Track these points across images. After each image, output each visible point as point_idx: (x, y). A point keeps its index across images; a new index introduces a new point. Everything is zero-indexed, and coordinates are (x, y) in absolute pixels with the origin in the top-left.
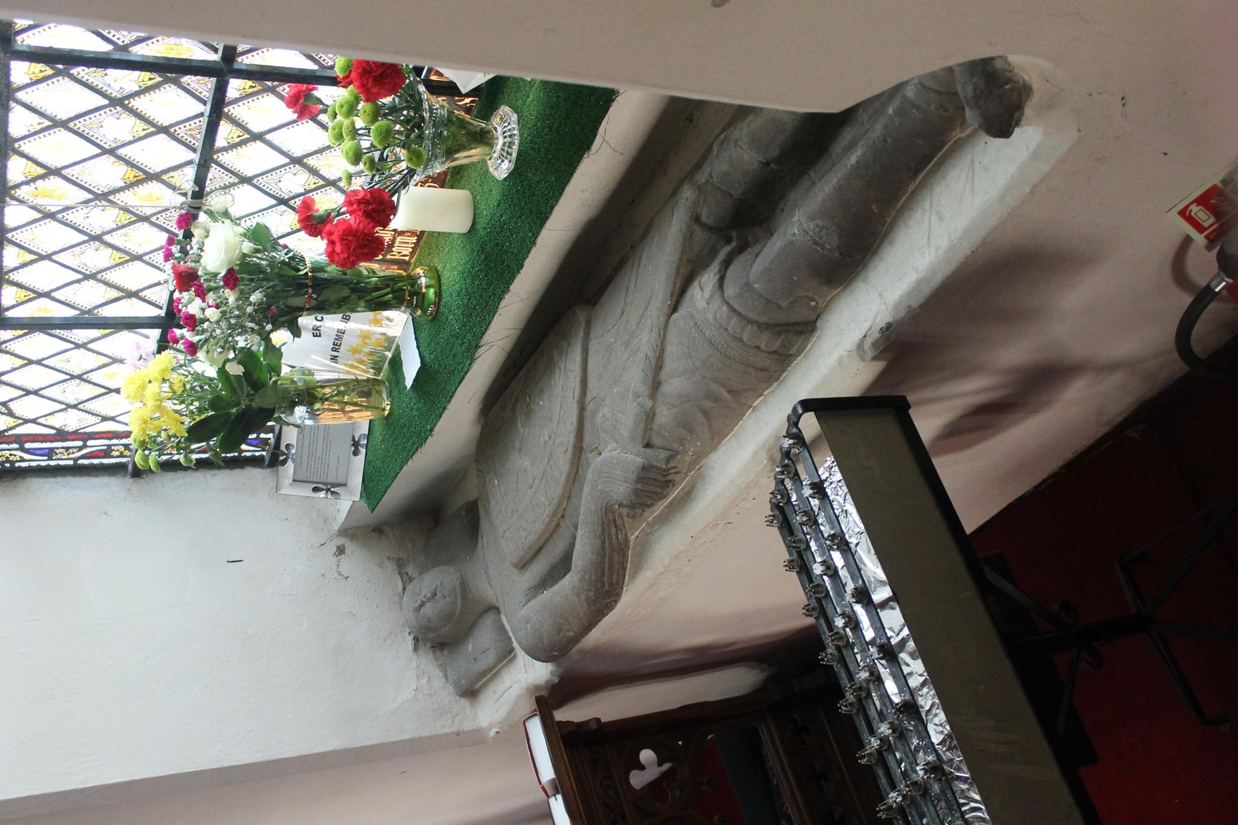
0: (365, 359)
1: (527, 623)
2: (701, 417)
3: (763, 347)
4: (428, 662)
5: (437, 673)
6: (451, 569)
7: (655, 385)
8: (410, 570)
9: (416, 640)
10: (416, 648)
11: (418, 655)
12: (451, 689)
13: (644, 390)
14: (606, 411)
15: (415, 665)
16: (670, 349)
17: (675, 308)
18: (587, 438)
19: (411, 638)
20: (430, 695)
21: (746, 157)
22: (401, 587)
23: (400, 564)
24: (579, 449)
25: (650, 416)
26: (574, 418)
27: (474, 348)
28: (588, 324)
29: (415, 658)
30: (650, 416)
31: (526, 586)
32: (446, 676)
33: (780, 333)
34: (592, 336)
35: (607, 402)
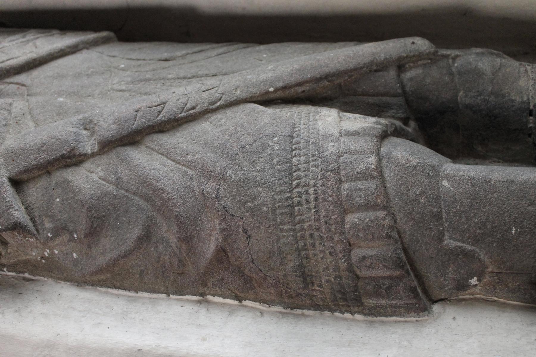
2: (136, 232)
3: (357, 253)
7: (132, 138)
13: (108, 128)
14: (19, 105)
16: (205, 128)
21: (522, 83)
25: (72, 159)
28: (106, 41)
30: (72, 159)
33: (399, 265)
34: (101, 49)
35: (33, 100)
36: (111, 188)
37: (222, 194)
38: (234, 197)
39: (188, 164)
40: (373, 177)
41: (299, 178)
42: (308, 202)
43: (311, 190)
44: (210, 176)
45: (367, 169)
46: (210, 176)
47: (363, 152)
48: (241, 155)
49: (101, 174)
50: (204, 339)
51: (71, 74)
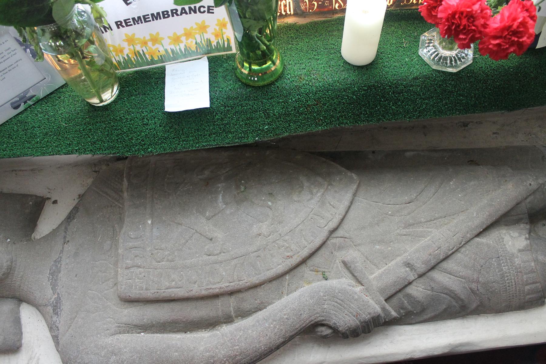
0: (126, 52)
17: (478, 235)
18: (317, 260)
24: (304, 261)
26: (318, 242)
31: (124, 320)
36: (429, 292)
37: (479, 288)
38: (484, 288)
39: (461, 277)
40: (534, 272)
41: (507, 276)
42: (512, 285)
43: (513, 281)
44: (473, 282)
45: (532, 269)
46: (473, 282)
47: (528, 261)
48: (482, 270)
49: (423, 287)
50: (471, 333)
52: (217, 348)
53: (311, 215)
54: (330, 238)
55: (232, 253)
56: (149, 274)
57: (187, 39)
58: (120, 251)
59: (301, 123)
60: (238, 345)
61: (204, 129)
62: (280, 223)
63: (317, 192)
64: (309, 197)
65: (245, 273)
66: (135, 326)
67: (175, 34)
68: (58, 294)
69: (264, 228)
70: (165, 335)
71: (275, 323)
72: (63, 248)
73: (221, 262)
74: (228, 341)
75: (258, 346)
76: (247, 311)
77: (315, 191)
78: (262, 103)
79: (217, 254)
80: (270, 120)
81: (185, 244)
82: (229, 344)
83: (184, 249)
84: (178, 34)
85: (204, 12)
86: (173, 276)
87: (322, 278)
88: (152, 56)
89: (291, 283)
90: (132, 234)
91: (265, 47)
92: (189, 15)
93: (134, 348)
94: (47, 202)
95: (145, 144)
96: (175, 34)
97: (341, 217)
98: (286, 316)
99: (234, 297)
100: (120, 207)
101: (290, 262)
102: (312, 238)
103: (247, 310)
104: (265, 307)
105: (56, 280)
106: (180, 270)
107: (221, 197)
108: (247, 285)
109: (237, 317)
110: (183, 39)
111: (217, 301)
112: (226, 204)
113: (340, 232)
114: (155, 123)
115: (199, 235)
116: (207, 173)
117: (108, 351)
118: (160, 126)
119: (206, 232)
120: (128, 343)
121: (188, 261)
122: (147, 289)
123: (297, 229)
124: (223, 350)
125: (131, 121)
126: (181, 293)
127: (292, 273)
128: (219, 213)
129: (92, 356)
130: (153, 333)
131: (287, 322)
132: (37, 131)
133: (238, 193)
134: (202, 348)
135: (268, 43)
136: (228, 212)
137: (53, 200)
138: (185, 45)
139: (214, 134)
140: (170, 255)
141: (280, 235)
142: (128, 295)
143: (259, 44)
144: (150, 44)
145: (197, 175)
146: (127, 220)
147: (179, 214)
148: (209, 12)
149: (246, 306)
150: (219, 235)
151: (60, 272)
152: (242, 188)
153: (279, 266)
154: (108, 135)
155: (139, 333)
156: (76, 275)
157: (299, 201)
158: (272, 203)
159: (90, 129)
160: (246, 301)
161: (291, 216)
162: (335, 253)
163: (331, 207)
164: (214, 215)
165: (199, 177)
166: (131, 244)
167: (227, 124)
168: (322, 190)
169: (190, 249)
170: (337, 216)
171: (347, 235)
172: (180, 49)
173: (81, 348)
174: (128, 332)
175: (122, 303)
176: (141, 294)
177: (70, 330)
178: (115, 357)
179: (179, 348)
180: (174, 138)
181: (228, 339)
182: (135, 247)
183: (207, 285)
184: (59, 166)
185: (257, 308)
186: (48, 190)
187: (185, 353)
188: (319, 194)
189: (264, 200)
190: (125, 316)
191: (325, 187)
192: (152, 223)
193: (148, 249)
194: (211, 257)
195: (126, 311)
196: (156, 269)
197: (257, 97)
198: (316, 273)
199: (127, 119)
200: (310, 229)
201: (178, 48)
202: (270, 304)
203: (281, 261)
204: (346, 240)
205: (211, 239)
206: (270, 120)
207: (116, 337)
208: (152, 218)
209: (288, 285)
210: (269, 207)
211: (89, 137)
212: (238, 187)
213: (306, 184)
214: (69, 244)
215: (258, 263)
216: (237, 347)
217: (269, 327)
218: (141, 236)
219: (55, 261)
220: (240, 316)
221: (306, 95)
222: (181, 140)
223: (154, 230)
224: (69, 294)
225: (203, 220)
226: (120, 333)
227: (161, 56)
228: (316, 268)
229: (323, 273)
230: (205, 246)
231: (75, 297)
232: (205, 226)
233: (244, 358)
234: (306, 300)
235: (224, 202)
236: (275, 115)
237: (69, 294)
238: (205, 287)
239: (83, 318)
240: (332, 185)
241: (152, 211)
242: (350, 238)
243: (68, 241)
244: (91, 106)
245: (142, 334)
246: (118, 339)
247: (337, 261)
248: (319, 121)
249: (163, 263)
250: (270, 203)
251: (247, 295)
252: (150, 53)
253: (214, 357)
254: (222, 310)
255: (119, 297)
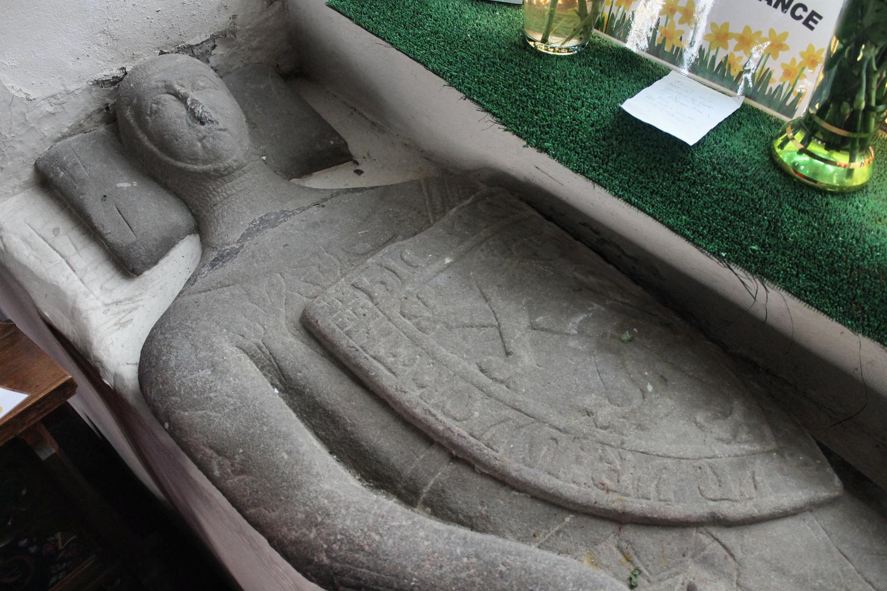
1: (213, 366)
4: (82, 104)
5: (66, 124)
6: (247, 142)
8: (219, 51)
9: (116, 81)
10: (97, 83)
11: (90, 91)
12: (43, 150)
15: (72, 88)
19: (119, 74)
20: (25, 124)
22: (192, 42)
23: (224, 37)
24: (620, 519)
26: (677, 510)
27: (761, 268)
29: (84, 85)
31: (277, 346)
32: (64, 137)
51: (794, 573)
52: (348, 508)
53: (702, 462)
54: (701, 529)
55: (520, 398)
56: (374, 319)
57: (737, 49)
58: (370, 260)
59: (821, 289)
60: (381, 535)
61: (653, 177)
62: (640, 427)
63: (746, 442)
64: (726, 436)
65: (509, 443)
66: (280, 369)
67: (726, 25)
68: (242, 246)
69: (606, 413)
70: (301, 425)
71: (474, 560)
72: (309, 207)
73: (489, 395)
74: (375, 514)
75: (409, 570)
76: (450, 509)
77: (744, 436)
78: (780, 206)
79: (495, 380)
80: (774, 242)
81: (465, 326)
82: (371, 521)
83: (456, 331)
84: (731, 30)
85: (800, 17)
86: (400, 350)
87: (626, 577)
88: (664, 40)
89: (564, 533)
90: (408, 254)
91: (863, 105)
92: (771, 8)
93: (245, 388)
94: (350, 163)
95: (547, 133)
96: (726, 25)
97: (756, 512)
98: (503, 568)
99: (455, 466)
100: (429, 222)
101: (598, 495)
102: (671, 496)
103: (453, 506)
104: (484, 531)
105: (258, 230)
106: (420, 349)
107: (581, 318)
108: (493, 462)
109: (427, 503)
110: (732, 43)
111: (423, 449)
112: (581, 332)
113: (730, 537)
114: (589, 116)
115: (498, 334)
116: (592, 279)
117: (211, 357)
118: (592, 125)
119: (511, 338)
120: (246, 376)
121: (443, 350)
122: (348, 333)
123: (659, 461)
124: (353, 520)
125: (558, 90)
126: (387, 381)
127: (583, 520)
128: (557, 333)
129: (188, 346)
130: (290, 405)
131: (494, 579)
132: (429, 23)
133: (613, 337)
134: (326, 487)
135: (873, 103)
136: (572, 343)
137: (360, 168)
138: (726, 57)
139: (661, 196)
140: (428, 319)
141: (623, 443)
142: (317, 317)
143: (860, 86)
144: (678, 16)
145: (576, 270)
146: (422, 236)
147: (499, 286)
148: (806, 23)
149: (459, 499)
150: (527, 358)
151: (273, 227)
152: (626, 336)
153: (574, 486)
154: (510, 85)
155: (274, 385)
156: (286, 245)
157: (701, 427)
158: (655, 391)
159: (494, 63)
160: (466, 490)
161: (668, 435)
162: (689, 561)
163: (751, 480)
164: (546, 330)
165: (575, 273)
166: (393, 263)
167: (695, 196)
168: (757, 447)
169: (464, 338)
170: (750, 504)
171: (739, 554)
172: (714, 58)
173: (189, 323)
174: (262, 369)
175: (299, 326)
176: (334, 331)
177: (203, 294)
178: (209, 373)
179: (298, 452)
180: (595, 157)
181: (378, 512)
182: (394, 272)
183: (436, 406)
184: (408, 142)
185: (470, 518)
186: (365, 154)
187: (297, 468)
188: (746, 447)
189: (645, 377)
190: (283, 343)
191: (768, 448)
192: (449, 265)
193: (408, 288)
194: (481, 374)
195: (290, 339)
196: (390, 320)
197: (778, 191)
198: (624, 560)
199: (555, 84)
200: (682, 480)
201: (713, 53)
202: (496, 532)
203: (583, 480)
204: (730, 559)
205: (508, 354)
206: (774, 242)
207: (243, 356)
208: (456, 260)
209: (558, 532)
210: (644, 392)
211: (484, 71)
212: (621, 329)
213: (737, 416)
214: (321, 209)
215: (545, 448)
216: (377, 538)
217: (458, 559)
218: (417, 267)
219: (283, 212)
220: (432, 507)
221: (871, 248)
222: (604, 166)
223: (443, 275)
224: (253, 257)
225: (524, 322)
226: (252, 357)
227: (678, 48)
228: (632, 552)
229: (637, 572)
230: (490, 354)
231: (255, 265)
232: (519, 330)
233: (368, 568)
234: (564, 578)
235: (579, 327)
236: (785, 239)
237: (253, 257)
238: (427, 406)
239: (233, 295)
240: (782, 456)
241: (466, 252)
242: (740, 564)
243: (323, 206)
244: (525, 40)
245: (276, 391)
246: (240, 360)
247: (680, 578)
248: (857, 310)
249: (408, 322)
250: (650, 388)
251: (478, 483)
252: (666, 32)
253: (328, 515)
254: (416, 469)
255: (305, 310)
